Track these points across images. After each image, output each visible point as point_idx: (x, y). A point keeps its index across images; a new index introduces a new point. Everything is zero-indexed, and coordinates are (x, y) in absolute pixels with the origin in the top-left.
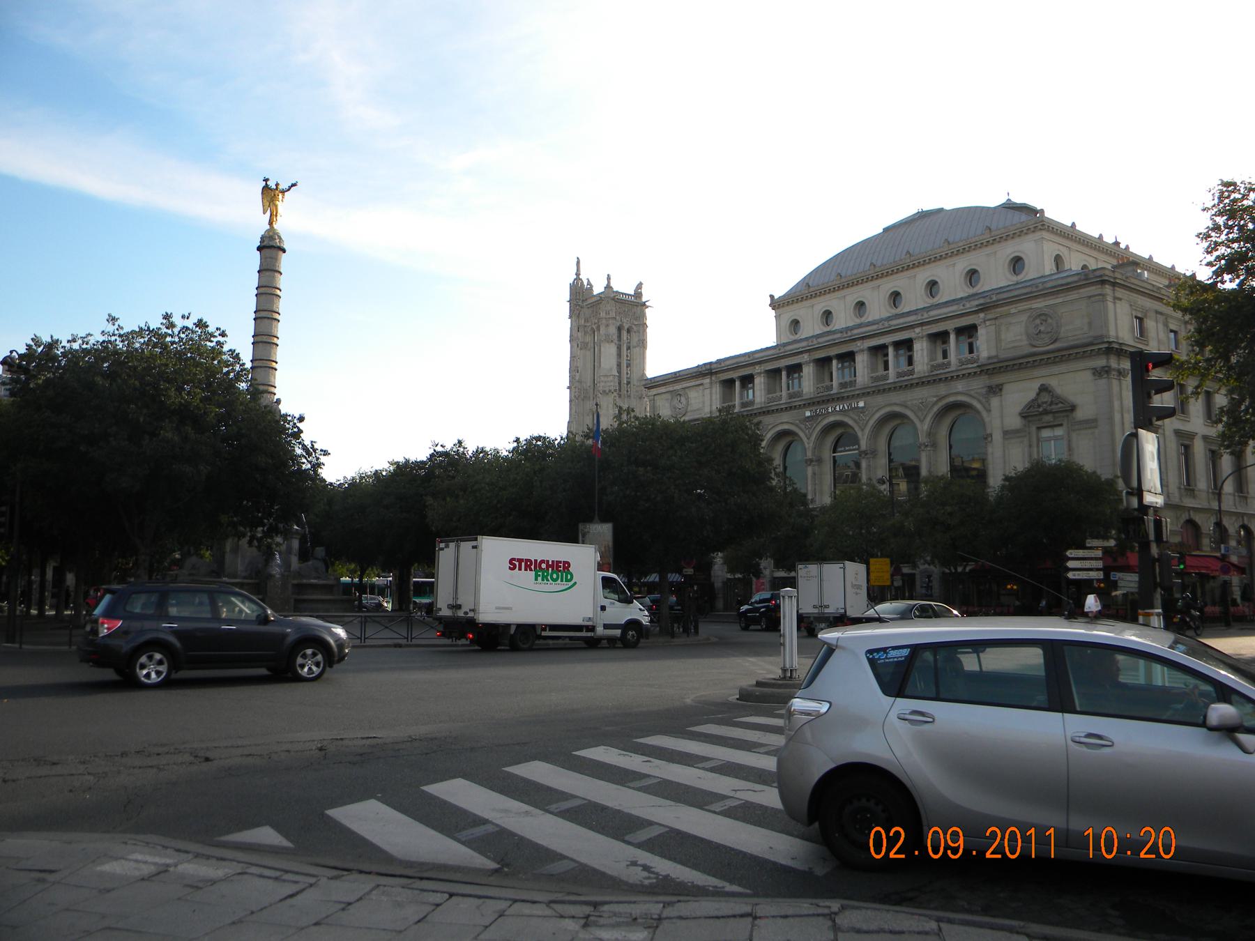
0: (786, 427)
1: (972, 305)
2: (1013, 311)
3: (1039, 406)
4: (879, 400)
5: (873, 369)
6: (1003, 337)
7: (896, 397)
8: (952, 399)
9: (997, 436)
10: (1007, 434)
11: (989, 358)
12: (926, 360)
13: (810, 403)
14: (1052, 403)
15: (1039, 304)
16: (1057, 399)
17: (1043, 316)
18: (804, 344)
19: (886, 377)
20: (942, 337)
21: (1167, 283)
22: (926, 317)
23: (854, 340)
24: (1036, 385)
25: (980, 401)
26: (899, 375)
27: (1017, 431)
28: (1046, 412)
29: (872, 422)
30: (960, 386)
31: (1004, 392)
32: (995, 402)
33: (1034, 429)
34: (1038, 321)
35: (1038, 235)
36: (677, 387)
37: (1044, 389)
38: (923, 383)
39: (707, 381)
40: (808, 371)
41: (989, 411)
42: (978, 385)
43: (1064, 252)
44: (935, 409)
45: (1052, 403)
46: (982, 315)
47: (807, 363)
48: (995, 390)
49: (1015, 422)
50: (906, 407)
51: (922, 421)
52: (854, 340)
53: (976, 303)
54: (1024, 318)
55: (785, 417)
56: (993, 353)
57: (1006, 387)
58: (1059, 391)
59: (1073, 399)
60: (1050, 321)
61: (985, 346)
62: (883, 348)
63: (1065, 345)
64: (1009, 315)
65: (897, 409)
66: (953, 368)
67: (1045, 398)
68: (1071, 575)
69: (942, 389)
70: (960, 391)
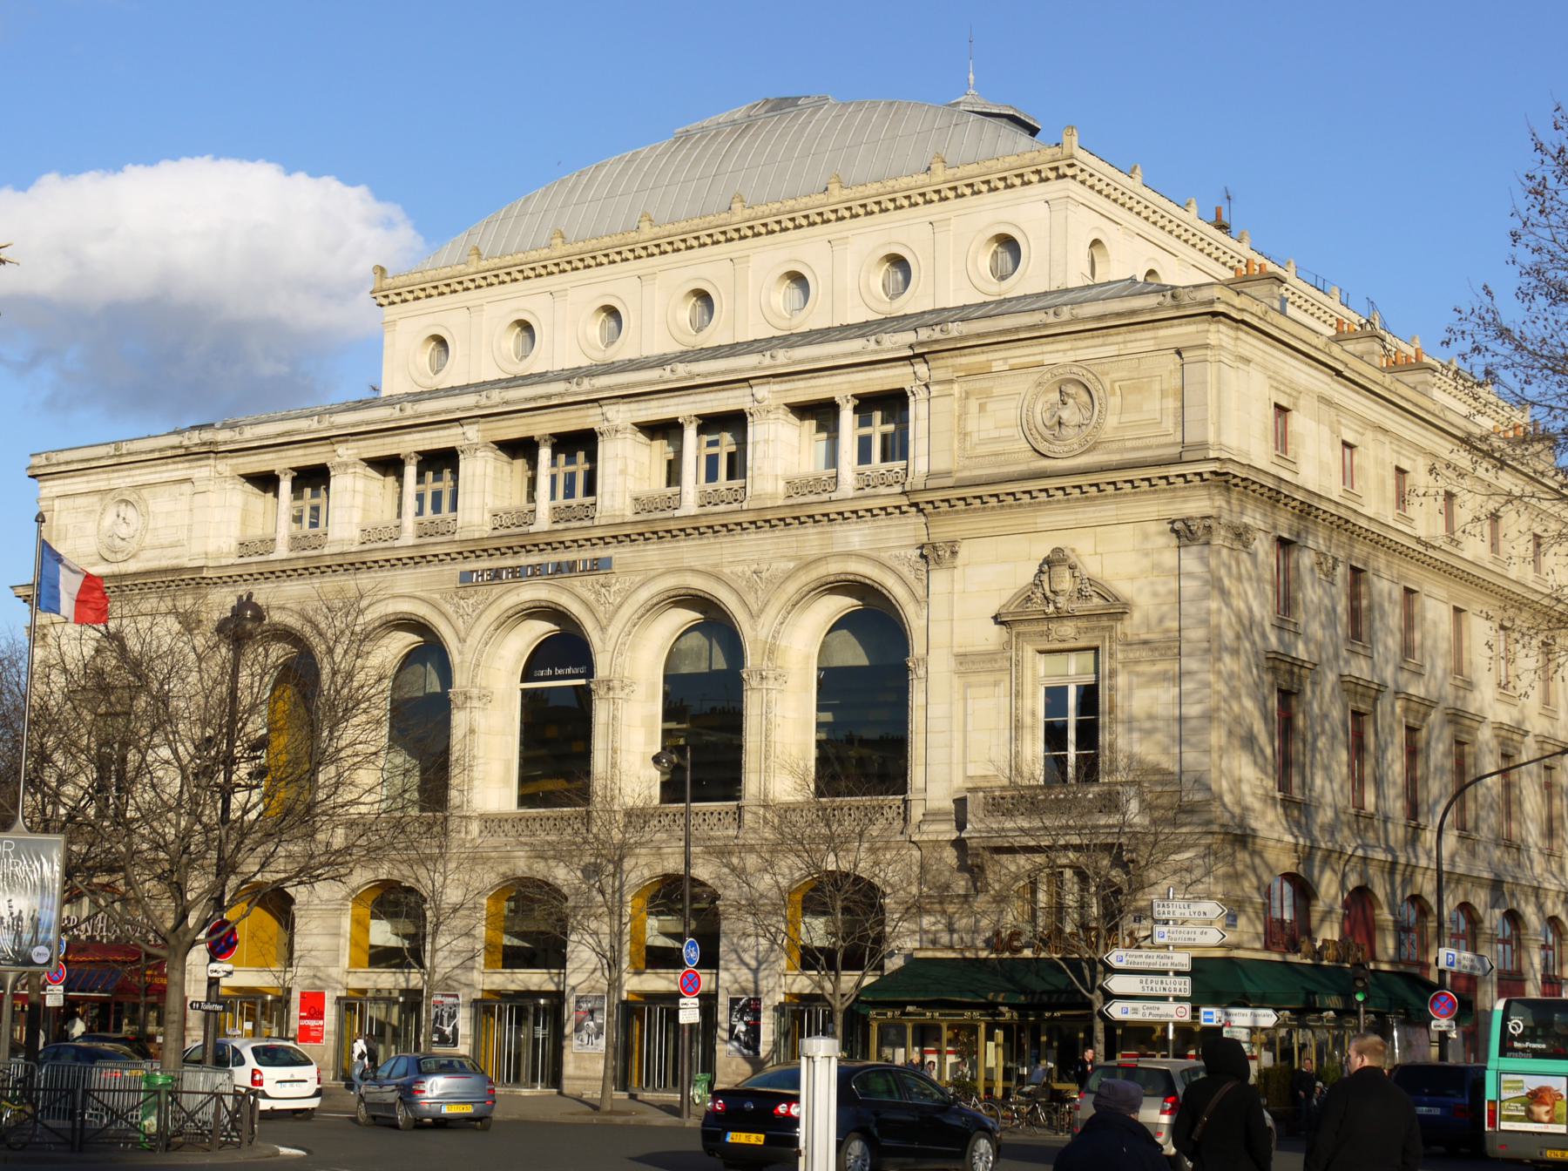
1: (896, 343)
2: (997, 366)
4: (653, 554)
6: (971, 425)
7: (691, 552)
10: (966, 661)
15: (1060, 354)
16: (1088, 587)
18: (469, 400)
19: (672, 503)
21: (1332, 332)
22: (784, 359)
27: (989, 656)
28: (1060, 616)
30: (855, 536)
31: (961, 559)
32: (939, 579)
35: (1055, 188)
36: (121, 480)
38: (765, 522)
39: (201, 471)
41: (924, 601)
42: (903, 535)
43: (1109, 233)
46: (921, 369)
47: (474, 448)
50: (718, 578)
53: (910, 337)
54: (1024, 384)
55: (405, 580)
57: (964, 550)
58: (1091, 566)
59: (1124, 589)
63: (1115, 458)
64: (986, 372)
68: (1117, 1011)
69: (811, 540)
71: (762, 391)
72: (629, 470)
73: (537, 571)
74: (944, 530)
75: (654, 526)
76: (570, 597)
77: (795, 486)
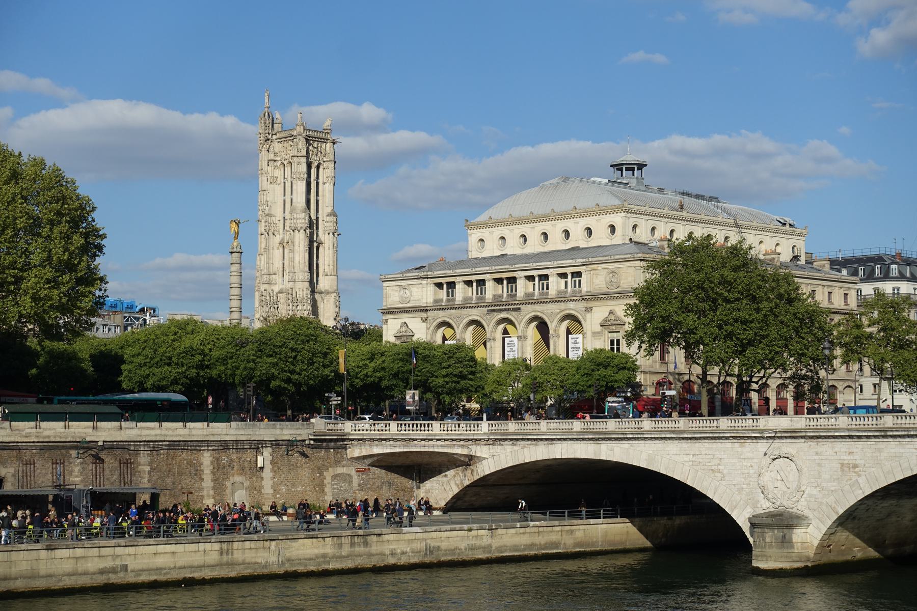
0: (475, 317)
4: (529, 307)
5: (526, 287)
7: (538, 307)
8: (567, 312)
19: (533, 294)
24: (608, 309)
29: (524, 320)
30: (571, 305)
32: (588, 315)
36: (404, 283)
37: (611, 313)
39: (424, 282)
41: (585, 320)
42: (582, 305)
44: (559, 316)
48: (588, 310)
55: (475, 311)
61: (587, 284)
67: (612, 317)
69: (562, 306)
70: (573, 308)
71: (551, 270)
72: (523, 287)
73: (504, 310)
74: (590, 304)
75: (529, 300)
76: (511, 316)
77: (559, 292)
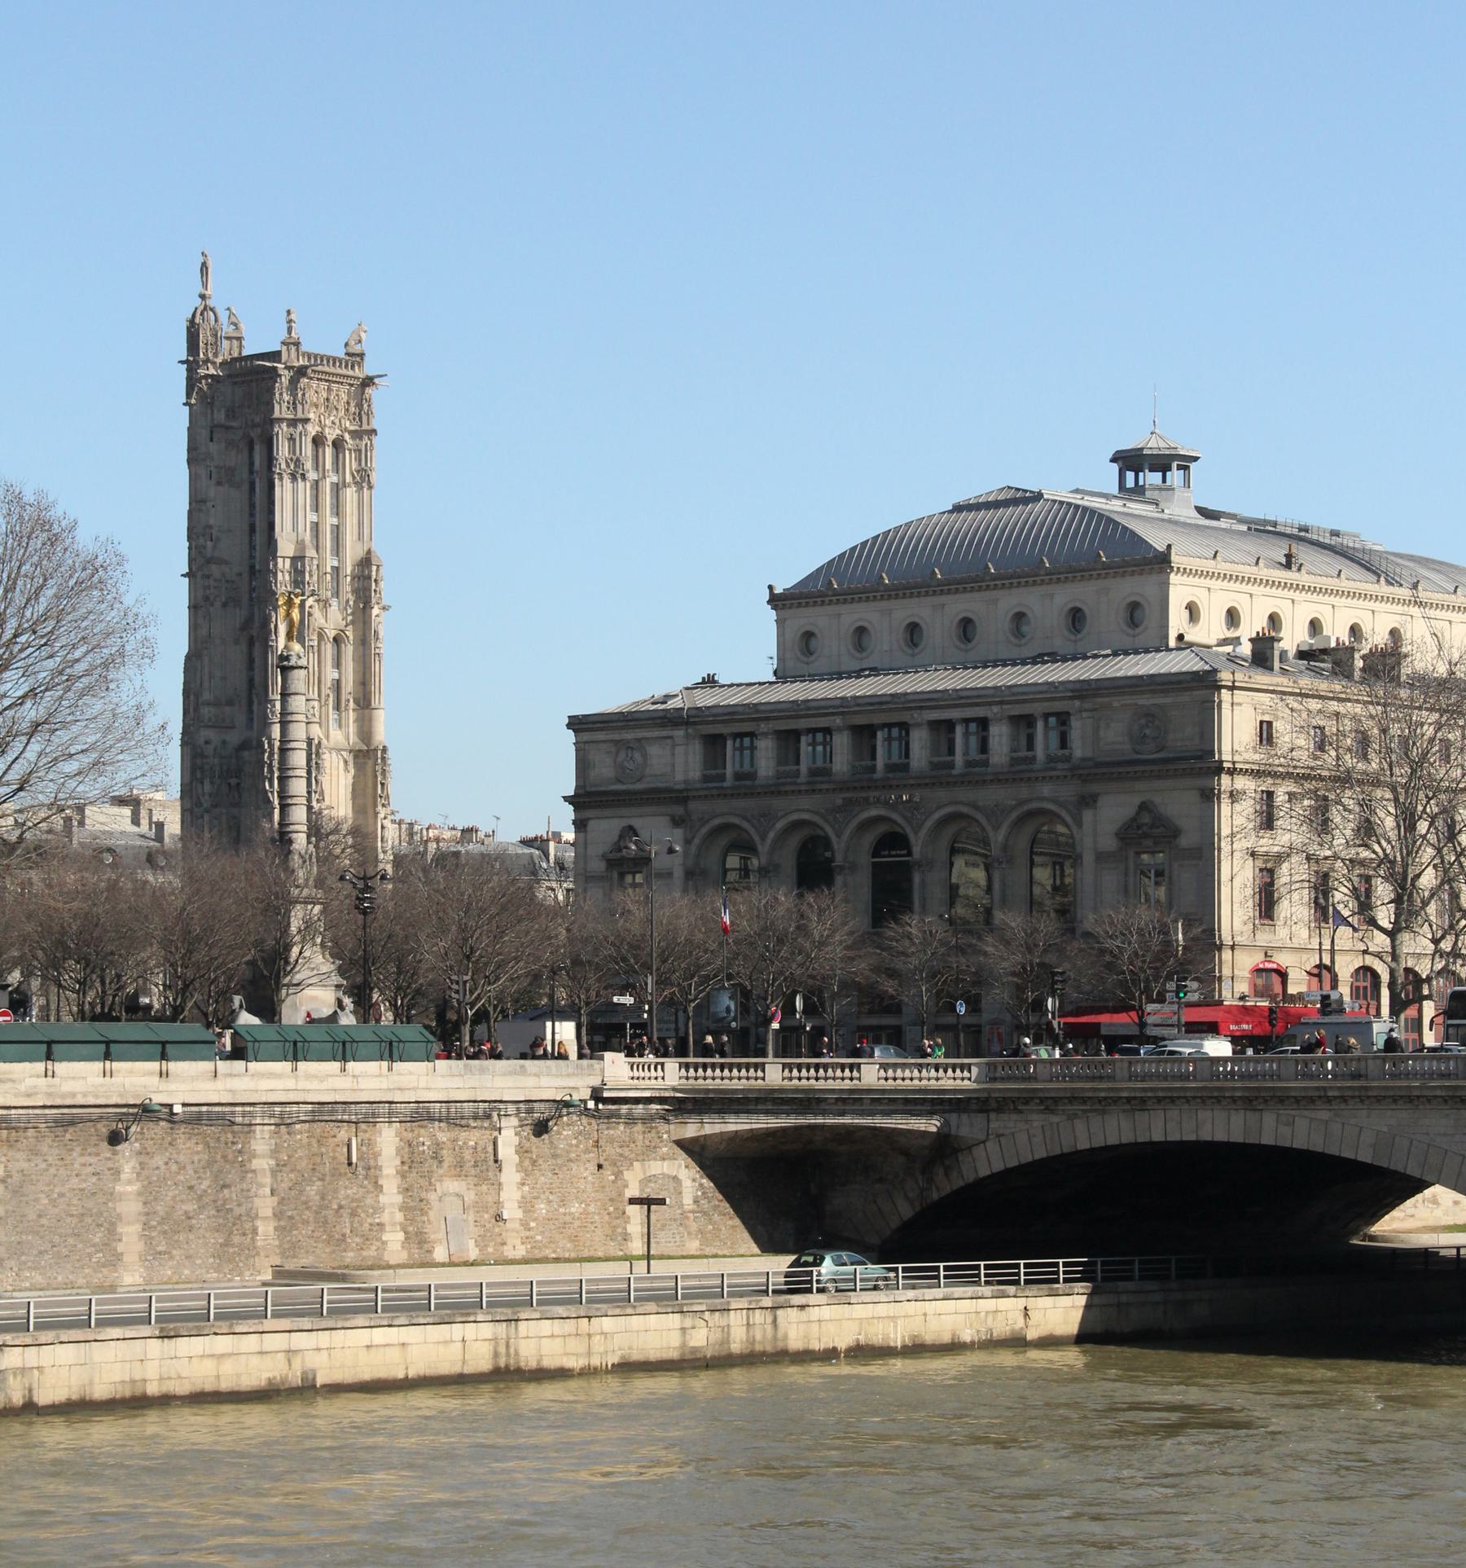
0: (805, 816)
3: (1139, 828)
4: (942, 794)
5: (935, 750)
6: (1102, 733)
7: (963, 794)
8: (1035, 805)
9: (1088, 858)
10: (1101, 857)
11: (1083, 759)
12: (1006, 749)
13: (843, 786)
14: (1152, 826)
15: (1145, 701)
17: (1149, 715)
20: (1028, 721)
23: (910, 709)
24: (1137, 800)
25: (1068, 811)
26: (969, 764)
29: (929, 823)
31: (1099, 804)
32: (1087, 816)
33: (1131, 853)
34: (1143, 721)
37: (1144, 807)
38: (999, 779)
40: (842, 743)
44: (1014, 815)
45: (1152, 826)
46: (1077, 703)
48: (1088, 801)
49: (1109, 843)
51: (996, 828)
52: (910, 709)
56: (1089, 754)
60: (1157, 722)
62: (950, 725)
65: (965, 810)
66: (1037, 766)
69: (1024, 792)
